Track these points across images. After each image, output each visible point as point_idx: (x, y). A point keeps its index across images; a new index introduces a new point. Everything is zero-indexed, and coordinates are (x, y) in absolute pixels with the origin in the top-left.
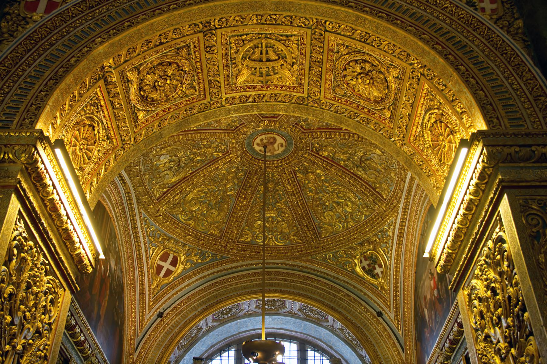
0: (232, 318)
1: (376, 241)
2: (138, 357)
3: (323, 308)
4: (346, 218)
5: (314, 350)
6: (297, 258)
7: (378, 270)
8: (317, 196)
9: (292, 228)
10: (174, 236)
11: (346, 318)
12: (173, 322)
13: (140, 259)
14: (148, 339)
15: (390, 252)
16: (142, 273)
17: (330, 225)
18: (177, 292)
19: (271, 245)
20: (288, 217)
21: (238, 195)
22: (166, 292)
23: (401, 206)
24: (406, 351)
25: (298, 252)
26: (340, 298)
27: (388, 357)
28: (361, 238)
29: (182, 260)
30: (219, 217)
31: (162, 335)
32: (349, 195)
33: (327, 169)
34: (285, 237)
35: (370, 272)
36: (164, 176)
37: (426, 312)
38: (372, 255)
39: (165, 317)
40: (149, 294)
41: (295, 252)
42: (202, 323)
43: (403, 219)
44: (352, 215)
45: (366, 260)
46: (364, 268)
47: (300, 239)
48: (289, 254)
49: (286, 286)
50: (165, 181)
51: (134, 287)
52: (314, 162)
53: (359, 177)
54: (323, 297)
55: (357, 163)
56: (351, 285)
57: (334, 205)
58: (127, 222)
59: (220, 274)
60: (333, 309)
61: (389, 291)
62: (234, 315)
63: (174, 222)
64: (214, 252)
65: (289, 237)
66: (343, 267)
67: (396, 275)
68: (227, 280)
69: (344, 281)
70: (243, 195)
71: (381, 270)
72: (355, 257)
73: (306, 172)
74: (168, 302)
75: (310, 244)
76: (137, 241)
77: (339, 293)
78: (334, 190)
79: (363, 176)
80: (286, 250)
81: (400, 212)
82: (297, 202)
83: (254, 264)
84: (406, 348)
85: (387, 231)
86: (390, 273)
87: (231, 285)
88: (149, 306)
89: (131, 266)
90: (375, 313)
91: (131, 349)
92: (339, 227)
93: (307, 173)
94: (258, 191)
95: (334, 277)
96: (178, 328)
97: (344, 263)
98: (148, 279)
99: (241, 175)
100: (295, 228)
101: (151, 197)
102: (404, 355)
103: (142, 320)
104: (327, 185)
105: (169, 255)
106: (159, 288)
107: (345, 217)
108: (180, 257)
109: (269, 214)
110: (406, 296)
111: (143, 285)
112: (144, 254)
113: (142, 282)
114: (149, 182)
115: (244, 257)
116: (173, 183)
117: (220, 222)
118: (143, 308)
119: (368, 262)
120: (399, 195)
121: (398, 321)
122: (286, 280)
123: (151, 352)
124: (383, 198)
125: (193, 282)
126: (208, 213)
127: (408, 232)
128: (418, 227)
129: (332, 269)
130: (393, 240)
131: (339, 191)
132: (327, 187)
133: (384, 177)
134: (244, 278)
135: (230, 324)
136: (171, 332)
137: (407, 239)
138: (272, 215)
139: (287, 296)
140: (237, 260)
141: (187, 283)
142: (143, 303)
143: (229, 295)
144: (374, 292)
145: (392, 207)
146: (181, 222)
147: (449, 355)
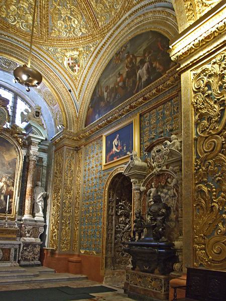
1: (82, 51)
7: (77, 68)
17: (59, 31)
23: (109, 34)
32: (78, 16)
35: (72, 68)
45: (72, 60)
46: (69, 64)
48: (27, 38)
69: (55, 67)
71: (79, 68)
78: (70, 9)
79: (94, 6)
83: (3, 34)
85: (91, 47)
109: (23, 4)
119: (72, 61)
122: (21, 53)
130: (93, 54)
132: (68, 3)
138: (24, 6)
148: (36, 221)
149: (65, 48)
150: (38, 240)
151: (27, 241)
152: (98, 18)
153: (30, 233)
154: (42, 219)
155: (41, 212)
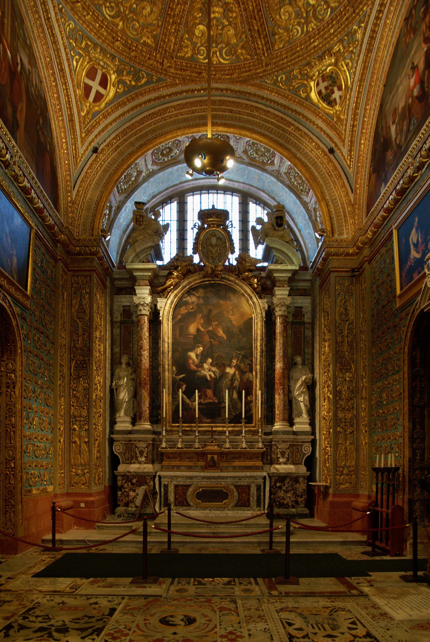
2: (76, 196)
3: (271, 144)
6: (245, 81)
9: (241, 37)
12: (110, 159)
20: (236, 18)
24: (356, 191)
25: (246, 72)
26: (290, 132)
27: (336, 199)
31: (99, 173)
39: (101, 153)
41: (243, 72)
47: (249, 54)
48: (235, 76)
49: (231, 118)
54: (271, 132)
56: (304, 116)
59: (157, 102)
60: (281, 145)
65: (236, 51)
68: (165, 110)
69: (296, 111)
74: (102, 135)
83: (195, 90)
84: (355, 187)
87: (170, 117)
90: (326, 150)
95: (285, 107)
97: (298, 87)
100: (243, 36)
102: (353, 195)
122: (231, 111)
123: (90, 192)
129: (283, 96)
134: (184, 108)
136: (109, 171)
139: (232, 130)
140: (177, 85)
143: (169, 129)
148: (295, 433)
149: (304, 62)
150: (303, 469)
151: (281, 471)
153: (286, 456)
154: (307, 428)
155: (305, 417)
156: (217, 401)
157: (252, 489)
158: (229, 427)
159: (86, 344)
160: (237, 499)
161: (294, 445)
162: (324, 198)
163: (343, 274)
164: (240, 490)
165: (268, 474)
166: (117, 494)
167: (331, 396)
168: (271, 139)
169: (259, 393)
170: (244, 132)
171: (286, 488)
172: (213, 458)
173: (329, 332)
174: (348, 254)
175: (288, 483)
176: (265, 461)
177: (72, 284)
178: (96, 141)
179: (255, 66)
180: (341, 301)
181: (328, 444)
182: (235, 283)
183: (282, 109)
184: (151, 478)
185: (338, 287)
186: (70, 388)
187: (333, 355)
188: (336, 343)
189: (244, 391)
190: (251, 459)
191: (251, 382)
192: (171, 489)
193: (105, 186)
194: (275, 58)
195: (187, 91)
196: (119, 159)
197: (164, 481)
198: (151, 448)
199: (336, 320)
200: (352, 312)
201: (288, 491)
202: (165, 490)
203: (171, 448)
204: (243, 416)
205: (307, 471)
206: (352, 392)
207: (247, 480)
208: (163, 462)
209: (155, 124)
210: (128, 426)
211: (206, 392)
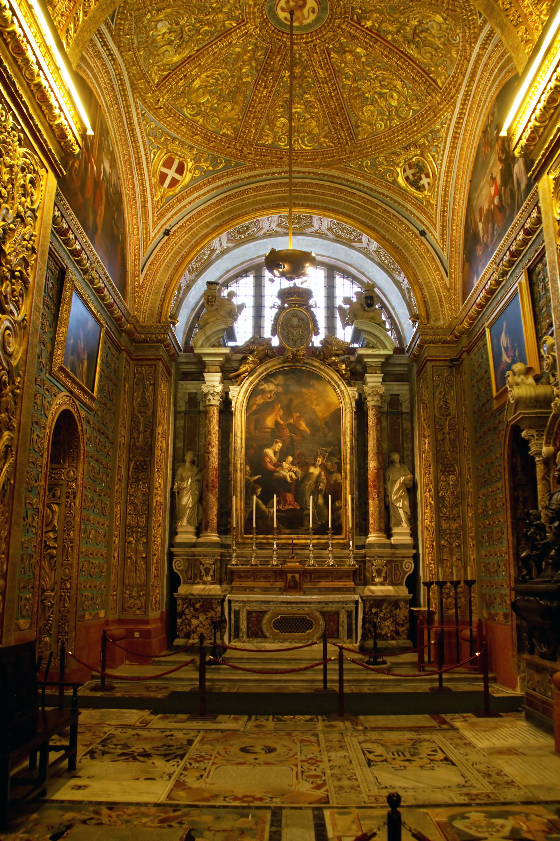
0: (250, 238)
1: (424, 144)
3: (357, 225)
4: (390, 115)
5: (344, 277)
6: (328, 166)
7: (425, 181)
8: (356, 85)
9: (323, 128)
10: (179, 136)
11: (384, 237)
12: (182, 241)
13: (139, 164)
14: (155, 259)
15: (441, 158)
16: (142, 182)
17: (369, 123)
18: (185, 206)
19: (296, 149)
20: (318, 113)
21: (256, 83)
22: (172, 206)
23: (461, 96)
24: (451, 274)
25: (330, 157)
27: (430, 282)
28: (408, 139)
29: (189, 167)
30: (233, 113)
31: (170, 255)
32: (395, 83)
33: (370, 45)
34: (314, 138)
35: (415, 183)
36: (163, 53)
37: (480, 225)
38: (419, 162)
39: (173, 235)
40: (153, 208)
41: (326, 158)
42: (215, 244)
43: (461, 114)
44: (397, 111)
46: (407, 179)
47: (332, 142)
48: (318, 161)
49: (315, 199)
50: (165, 61)
51: (134, 199)
52: (354, 36)
53: (409, 58)
54: (357, 213)
55: (409, 37)
56: (392, 199)
57: (376, 96)
58: (121, 115)
59: (236, 184)
60: (369, 227)
61: (436, 205)
62: (252, 235)
63: (178, 118)
64: (227, 158)
65: (318, 139)
66: (383, 177)
67: (446, 186)
68: (243, 192)
69: (383, 195)
70: (262, 82)
71: (428, 180)
72: (398, 165)
73: (342, 51)
74: (175, 217)
75: (344, 148)
76: (135, 141)
77: (376, 208)
78: (377, 77)
79: (416, 56)
80: (315, 155)
81: (458, 105)
82: (330, 93)
83: (276, 173)
85: (439, 131)
86: (438, 183)
87: (249, 198)
88: (154, 222)
89: (129, 172)
90: (418, 233)
91: (136, 270)
92: (381, 126)
93: (344, 53)
94: (282, 78)
95: (371, 189)
96: (188, 247)
98: (151, 190)
99: (261, 55)
100: (326, 127)
101: (149, 82)
103: (146, 238)
104: (369, 69)
105: (173, 160)
106: (164, 200)
107: (389, 112)
108: (187, 163)
110: (456, 211)
111: (144, 196)
112: (144, 158)
113: (144, 192)
114: (144, 61)
115: (264, 164)
116: (175, 64)
117: (235, 119)
118: (147, 223)
119: (413, 171)
120: (459, 81)
121: (444, 241)
122: (314, 193)
123: (159, 275)
124: (438, 86)
125: (204, 194)
126: (220, 106)
127: (466, 130)
128: (480, 123)
129: (369, 180)
130: (445, 142)
131: (384, 78)
132: (369, 72)
133: (442, 57)
134: (264, 190)
135: (247, 246)
136: (179, 253)
137: (464, 140)
138: (298, 110)
139: (315, 211)
140: (256, 168)
141: (196, 195)
142: (146, 218)
143: (247, 210)
144: (418, 208)
145: (448, 98)
146: (187, 117)
147: (506, 271)
150: (403, 591)
152: (432, 72)
153: (383, 574)
156: (298, 508)
157: (341, 616)
158: (314, 539)
159: (147, 442)
160: (323, 629)
161: (392, 561)
162: (417, 282)
163: (441, 363)
164: (327, 618)
165: (362, 597)
166: (176, 622)
167: (433, 502)
168: (357, 220)
169: (349, 497)
170: (327, 214)
171: (384, 614)
172: (293, 577)
173: (428, 427)
174: (445, 342)
175: (386, 608)
176: (358, 581)
177: (135, 374)
178: (168, 223)
179: (338, 153)
180: (441, 393)
181: (432, 560)
182: (320, 369)
183: (368, 191)
184: (218, 602)
185: (436, 378)
186: (127, 493)
187: (433, 455)
188: (437, 441)
189: (330, 496)
190: (340, 578)
191: (340, 485)
192: (243, 616)
193: (177, 270)
194: (359, 147)
195: (267, 174)
196: (192, 240)
197: (235, 606)
198: (219, 564)
199: (435, 415)
200: (453, 405)
201: (386, 619)
202: (235, 617)
203: (242, 565)
204: (330, 526)
205: (409, 593)
206: (457, 497)
207: (335, 605)
208: (234, 583)
209: (232, 205)
210: (192, 538)
211: (285, 496)
